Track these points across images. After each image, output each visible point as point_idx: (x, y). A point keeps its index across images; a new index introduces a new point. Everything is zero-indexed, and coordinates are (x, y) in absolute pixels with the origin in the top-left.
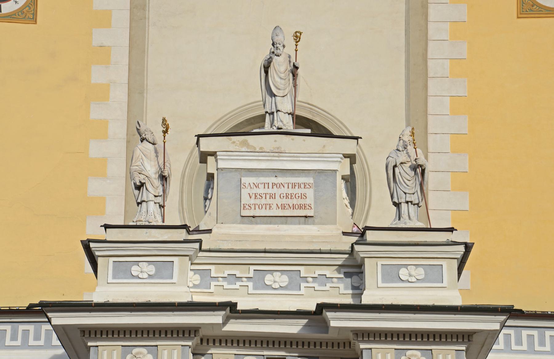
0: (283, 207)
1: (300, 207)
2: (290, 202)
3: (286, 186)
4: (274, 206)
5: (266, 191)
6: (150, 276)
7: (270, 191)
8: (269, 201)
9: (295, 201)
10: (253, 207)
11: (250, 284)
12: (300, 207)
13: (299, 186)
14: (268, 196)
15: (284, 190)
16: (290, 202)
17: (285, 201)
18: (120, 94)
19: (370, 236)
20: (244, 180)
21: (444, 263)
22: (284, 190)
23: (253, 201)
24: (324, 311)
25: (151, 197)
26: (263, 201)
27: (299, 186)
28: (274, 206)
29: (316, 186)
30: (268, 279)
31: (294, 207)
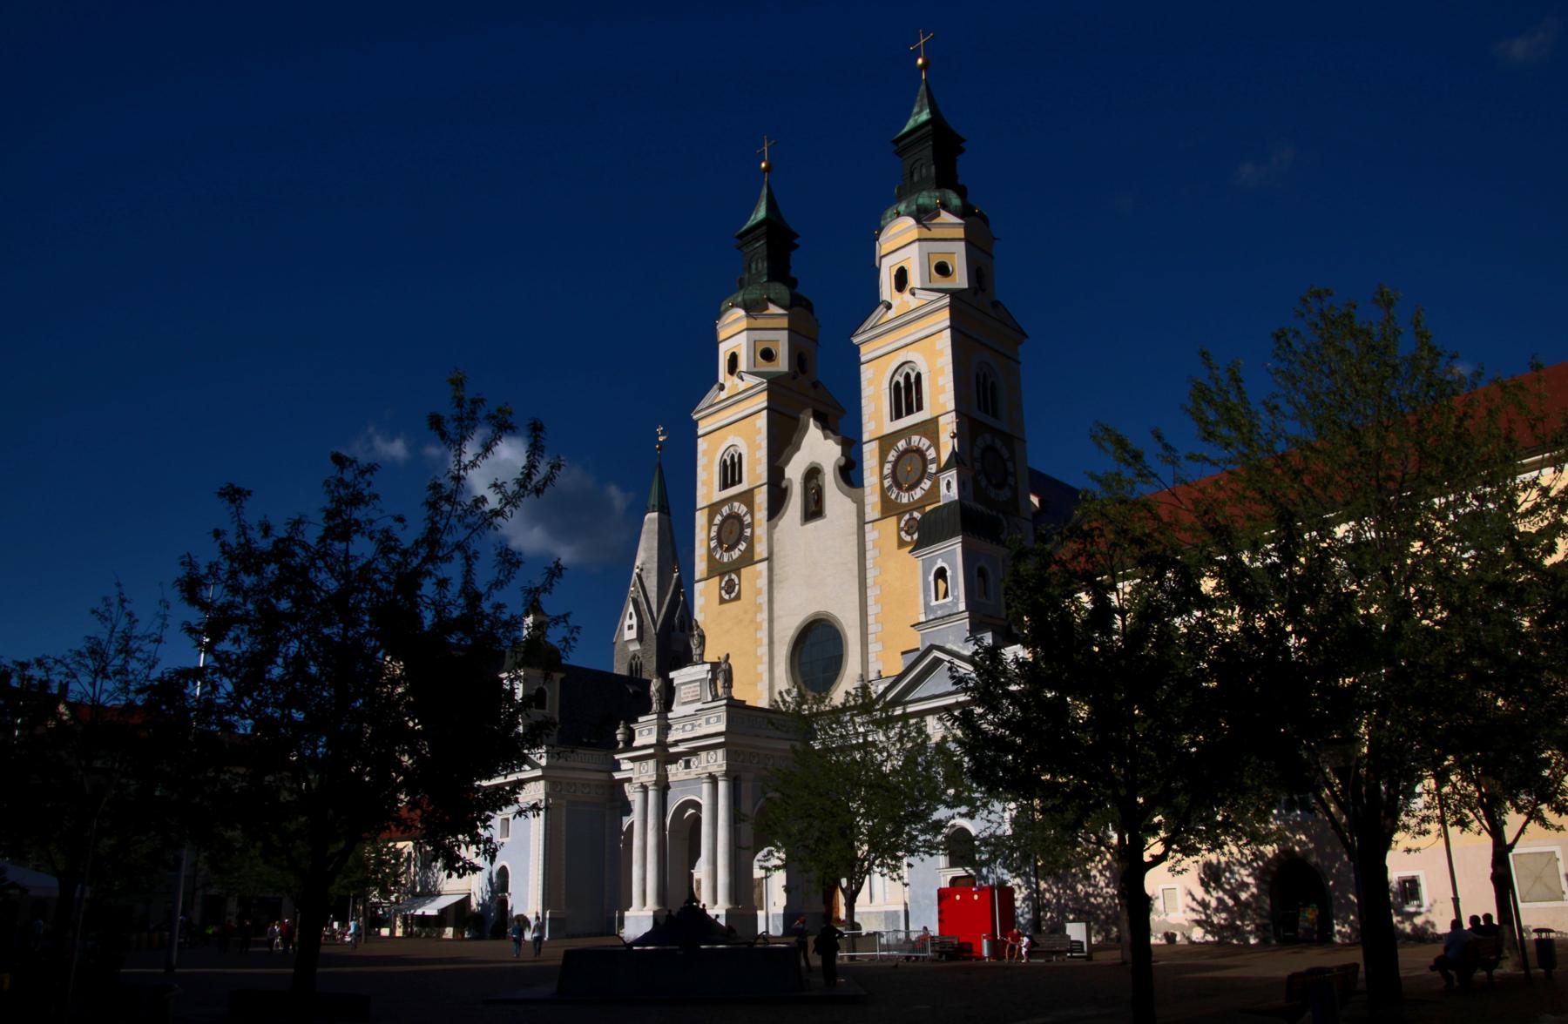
18: (765, 625)
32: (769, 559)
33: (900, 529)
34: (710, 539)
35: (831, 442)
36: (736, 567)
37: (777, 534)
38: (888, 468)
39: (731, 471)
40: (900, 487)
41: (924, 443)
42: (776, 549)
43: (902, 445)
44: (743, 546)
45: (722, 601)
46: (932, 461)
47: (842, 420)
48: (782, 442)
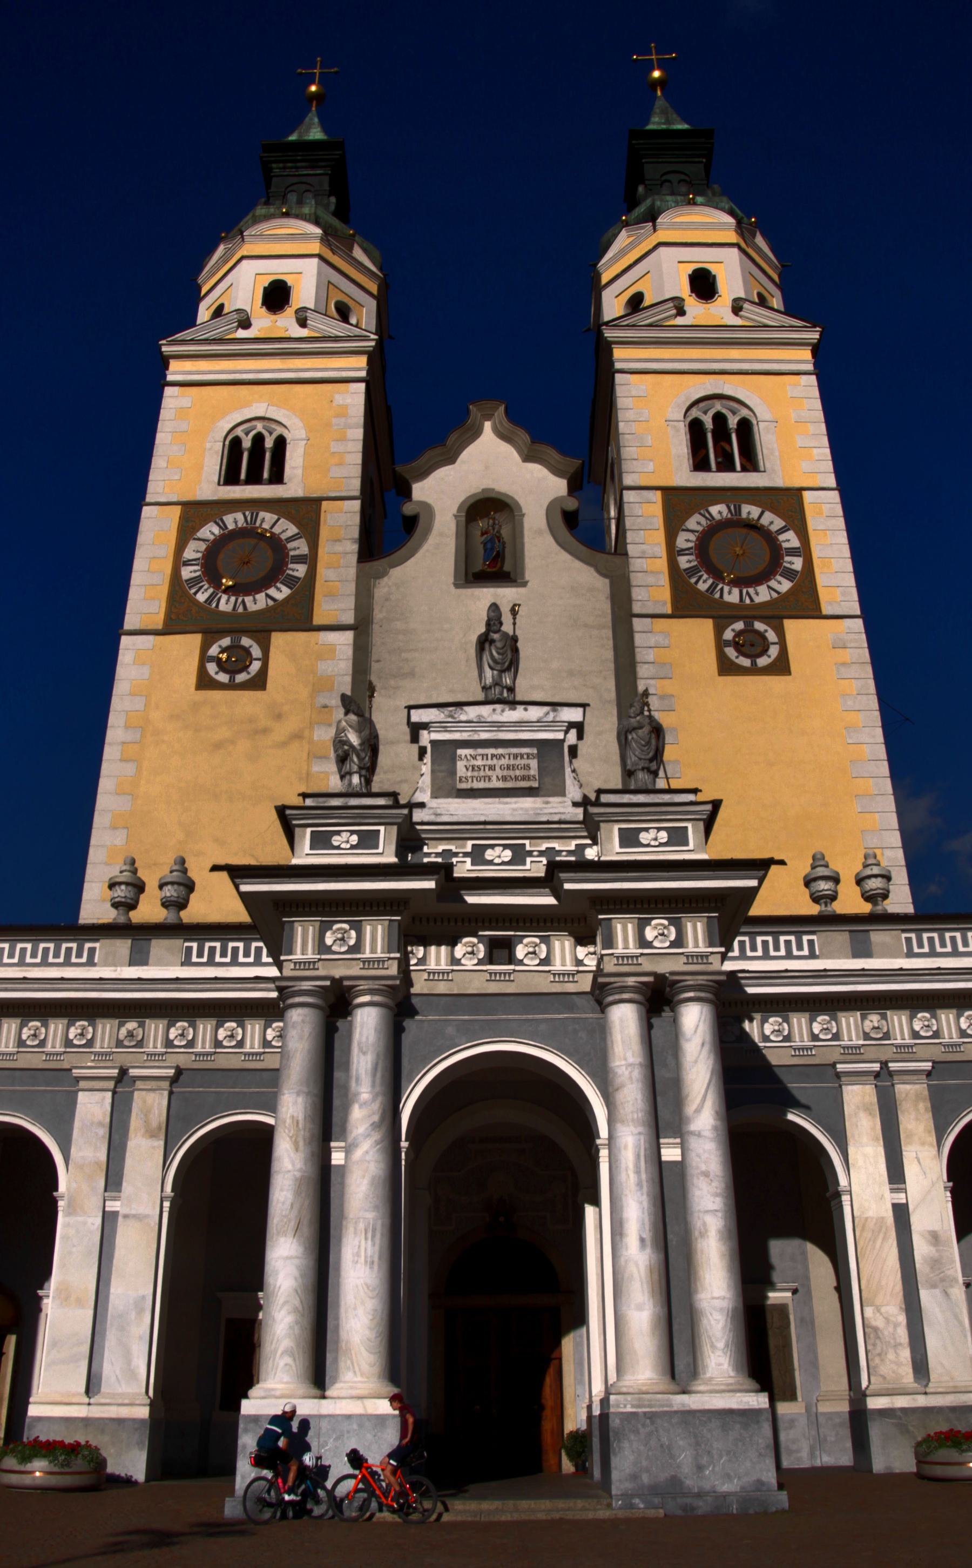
0: (504, 779)
1: (524, 778)
2: (512, 773)
3: (507, 757)
4: (494, 778)
5: (485, 762)
6: (353, 847)
7: (490, 762)
8: (489, 773)
9: (518, 773)
10: (470, 780)
11: (468, 860)
12: (524, 778)
13: (522, 757)
14: (487, 768)
15: (504, 762)
16: (512, 773)
17: (505, 773)
19: (604, 798)
20: (459, 752)
21: (689, 825)
22: (504, 762)
23: (469, 774)
24: (556, 871)
25: (355, 768)
26: (482, 773)
27: (522, 757)
28: (494, 778)
29: (540, 757)
30: (489, 854)
31: (516, 778)
32: (362, 627)
33: (720, 645)
34: (179, 562)
35: (537, 471)
36: (263, 627)
37: (382, 589)
38: (684, 540)
39: (256, 457)
40: (717, 575)
41: (773, 521)
42: (378, 615)
43: (718, 510)
44: (281, 593)
45: (204, 682)
46: (793, 552)
47: (580, 434)
48: (400, 440)
